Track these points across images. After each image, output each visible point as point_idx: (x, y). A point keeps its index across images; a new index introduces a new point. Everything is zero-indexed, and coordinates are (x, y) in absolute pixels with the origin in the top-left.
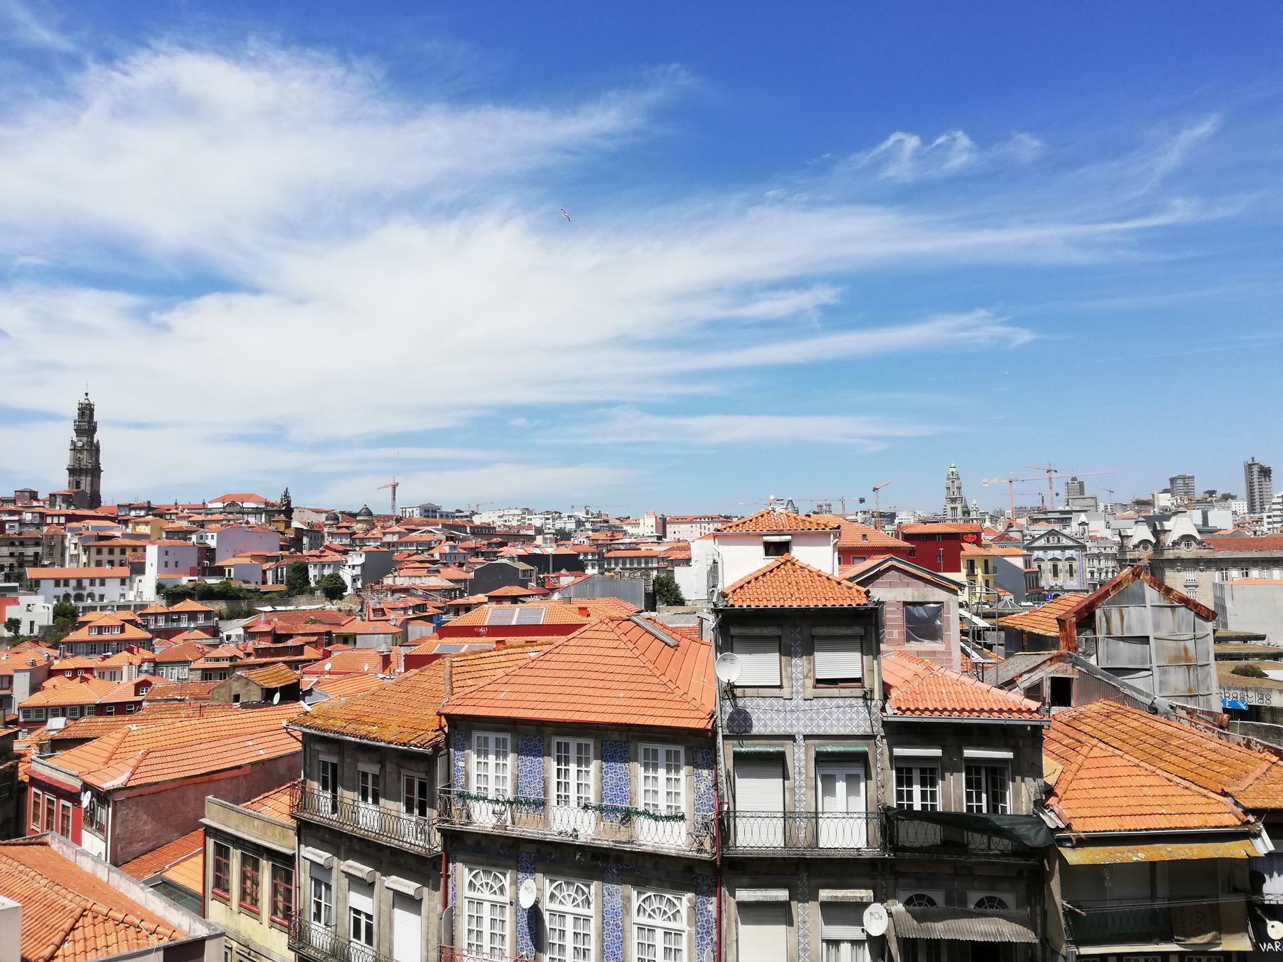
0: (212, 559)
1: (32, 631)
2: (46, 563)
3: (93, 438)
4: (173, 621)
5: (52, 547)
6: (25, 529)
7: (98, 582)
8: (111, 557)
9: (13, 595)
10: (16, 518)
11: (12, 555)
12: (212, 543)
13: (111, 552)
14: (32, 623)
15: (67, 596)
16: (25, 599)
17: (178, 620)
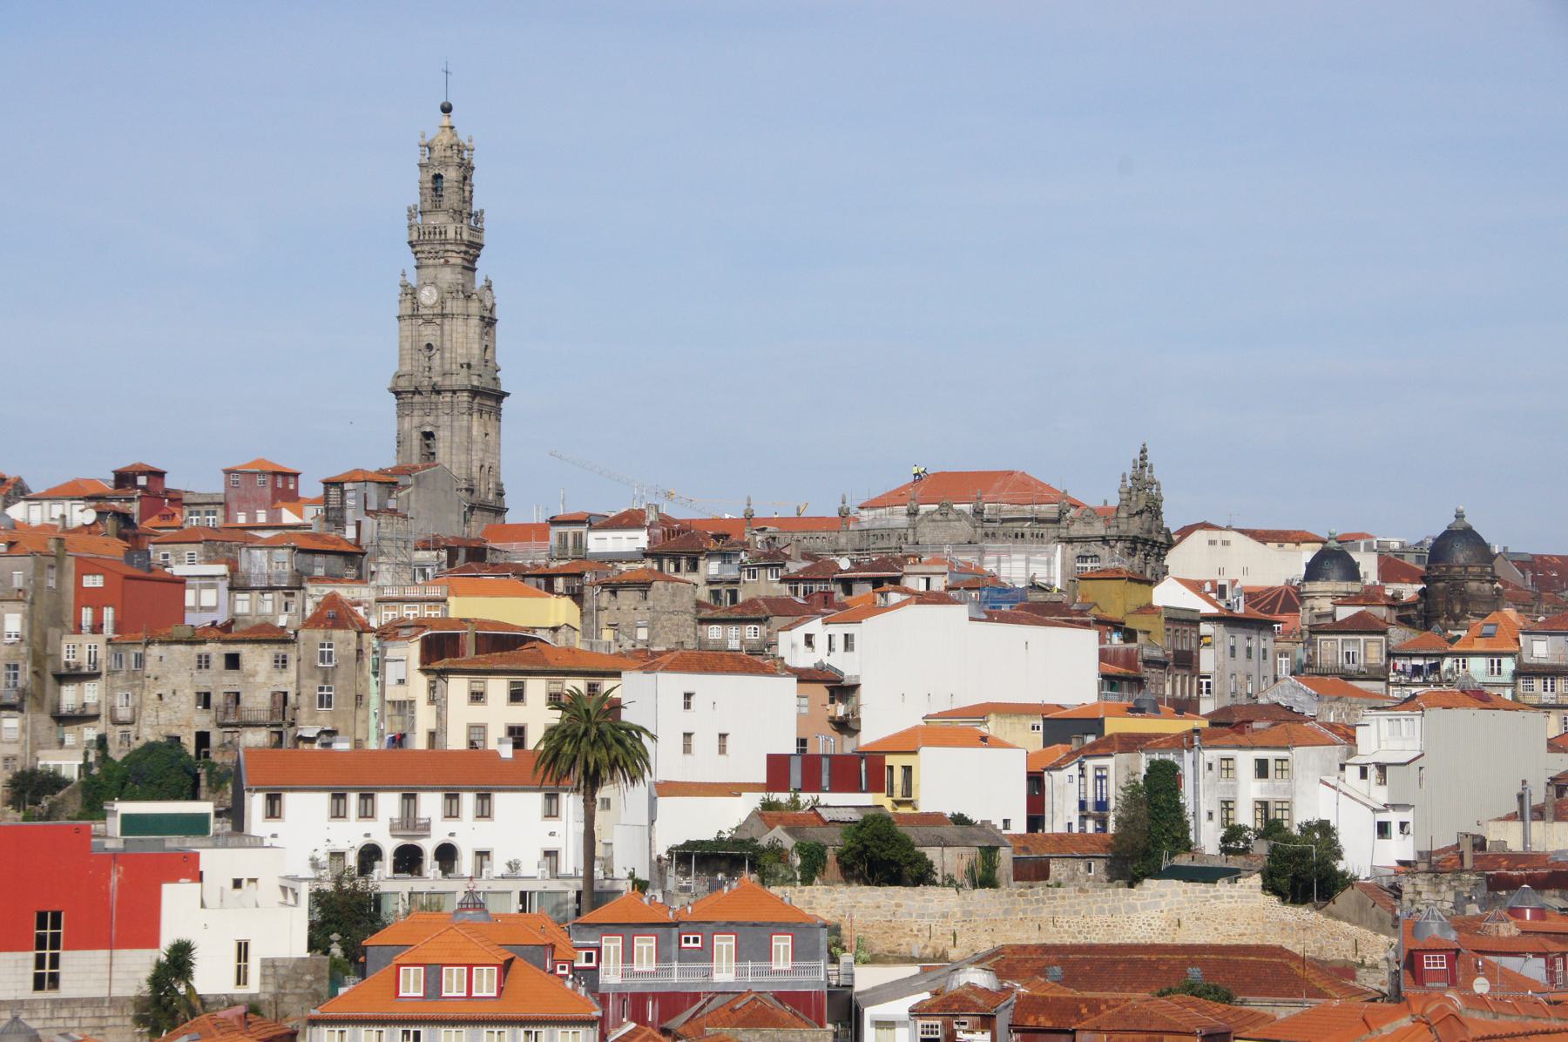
0: (846, 726)
1: (241, 978)
2: (310, 732)
3: (470, 267)
4: (685, 956)
5: (327, 675)
6: (243, 604)
7: (468, 800)
8: (516, 715)
9: (190, 843)
10: (222, 569)
11: (205, 700)
12: (847, 665)
13: (517, 696)
14: (243, 950)
15: (370, 855)
16: (217, 861)
17: (706, 954)
